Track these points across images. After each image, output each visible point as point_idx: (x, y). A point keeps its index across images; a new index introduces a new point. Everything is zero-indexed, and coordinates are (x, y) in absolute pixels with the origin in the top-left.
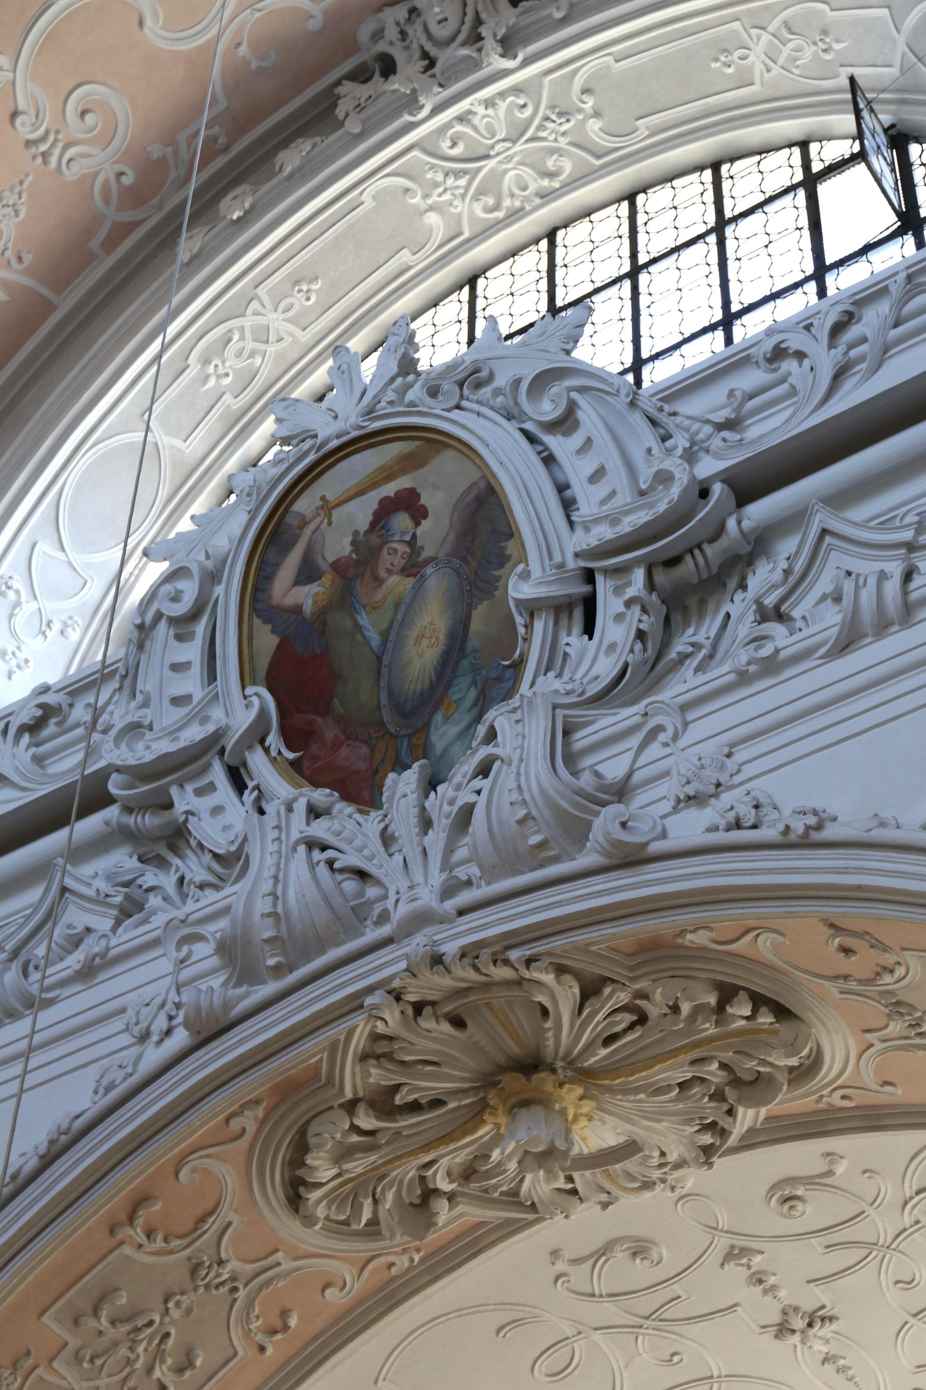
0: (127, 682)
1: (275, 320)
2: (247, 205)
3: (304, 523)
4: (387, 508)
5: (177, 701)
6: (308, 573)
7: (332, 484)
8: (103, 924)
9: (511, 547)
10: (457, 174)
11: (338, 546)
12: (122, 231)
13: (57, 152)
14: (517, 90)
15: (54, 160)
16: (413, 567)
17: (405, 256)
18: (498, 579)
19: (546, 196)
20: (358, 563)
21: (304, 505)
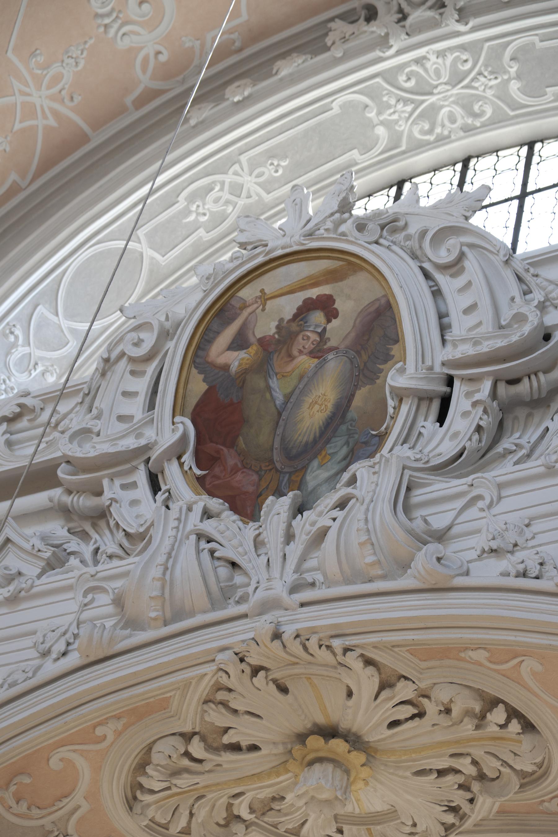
0: (88, 399)
1: (249, 182)
2: (246, 93)
3: (245, 306)
4: (308, 306)
5: (121, 418)
6: (239, 342)
7: (271, 282)
8: (31, 570)
9: (395, 350)
10: (406, 101)
11: (266, 327)
12: (150, 95)
13: (116, 26)
14: (462, 48)
15: (112, 32)
16: (319, 352)
17: (355, 154)
18: (381, 371)
19: (468, 130)
20: (279, 341)
21: (247, 293)
